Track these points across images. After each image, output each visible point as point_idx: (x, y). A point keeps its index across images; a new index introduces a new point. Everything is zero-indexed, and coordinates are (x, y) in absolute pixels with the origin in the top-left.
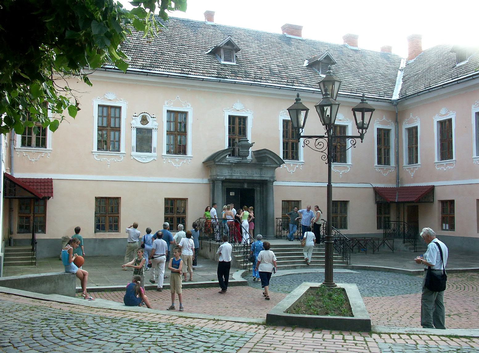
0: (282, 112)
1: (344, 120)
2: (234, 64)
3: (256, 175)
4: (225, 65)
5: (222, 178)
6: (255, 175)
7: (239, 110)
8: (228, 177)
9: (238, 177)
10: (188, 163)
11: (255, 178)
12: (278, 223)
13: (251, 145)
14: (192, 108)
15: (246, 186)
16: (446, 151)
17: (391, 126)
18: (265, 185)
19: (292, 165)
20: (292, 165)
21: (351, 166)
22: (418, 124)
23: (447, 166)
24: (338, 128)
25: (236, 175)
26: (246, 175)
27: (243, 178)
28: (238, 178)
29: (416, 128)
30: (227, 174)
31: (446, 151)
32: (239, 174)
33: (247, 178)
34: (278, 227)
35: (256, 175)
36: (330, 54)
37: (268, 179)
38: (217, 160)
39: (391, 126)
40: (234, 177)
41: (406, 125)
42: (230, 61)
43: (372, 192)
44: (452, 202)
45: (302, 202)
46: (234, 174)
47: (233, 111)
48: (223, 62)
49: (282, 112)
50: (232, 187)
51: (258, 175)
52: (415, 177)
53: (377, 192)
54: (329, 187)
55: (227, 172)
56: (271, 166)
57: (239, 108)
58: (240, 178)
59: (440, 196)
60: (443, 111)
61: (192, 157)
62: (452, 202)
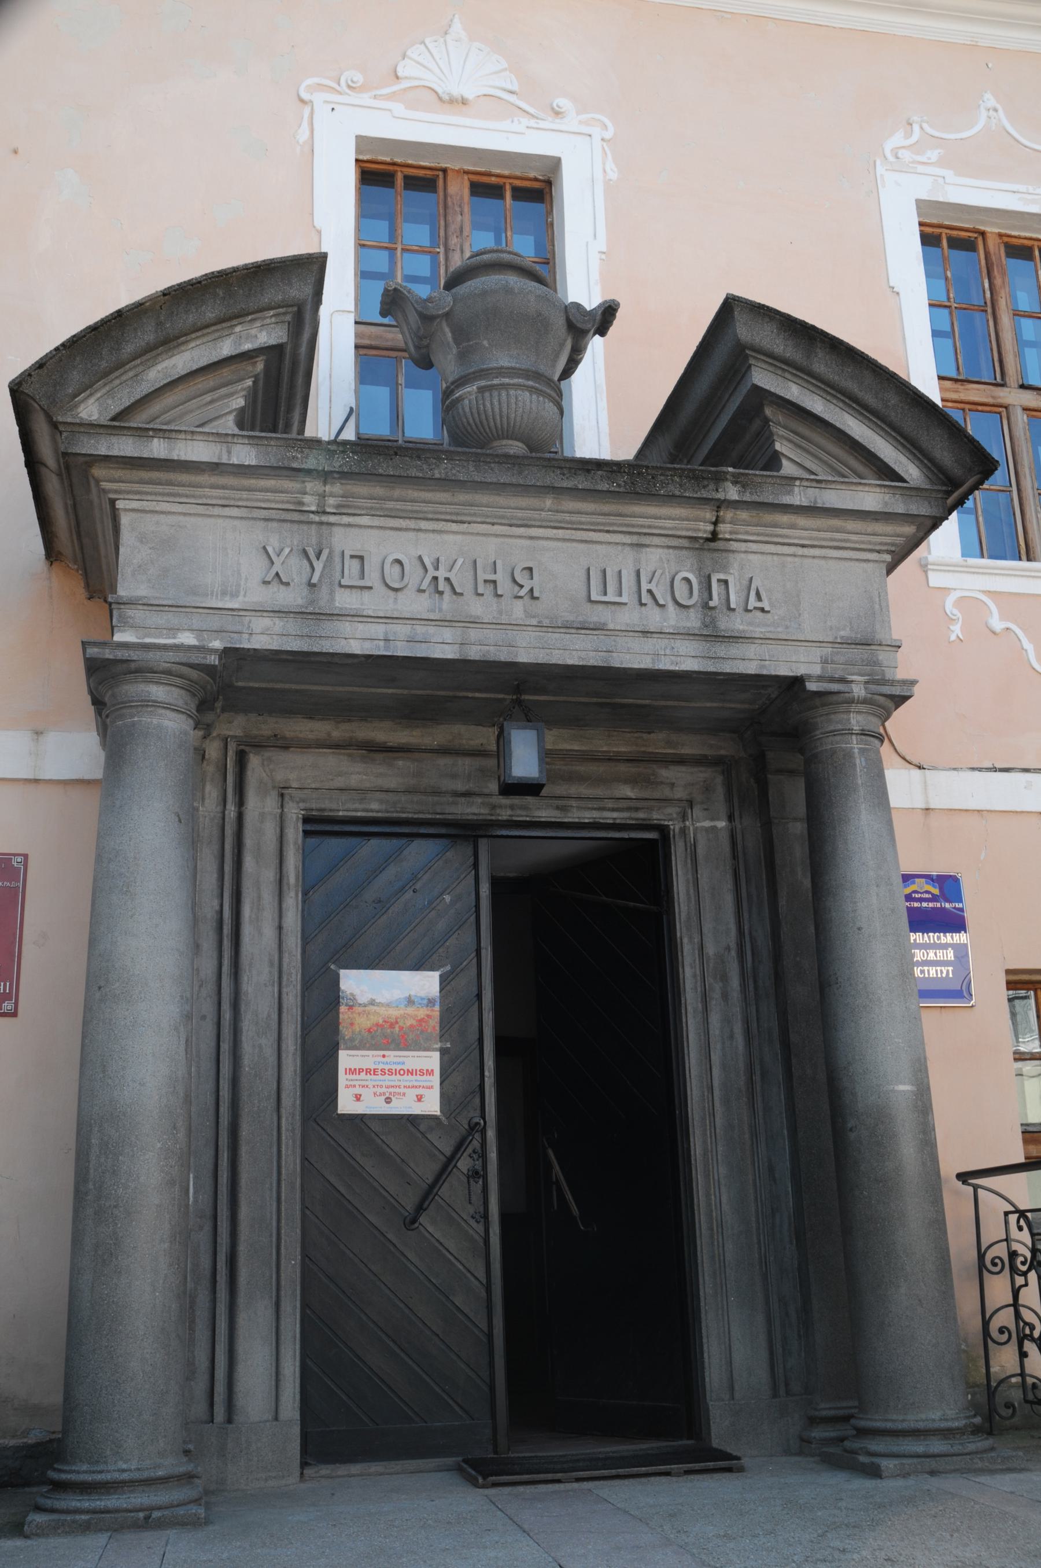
0: (897, 139)
5: (187, 639)
6: (604, 597)
7: (464, 102)
8: (264, 635)
9: (402, 630)
11: (635, 655)
12: (993, 1231)
27: (474, 653)
28: (401, 650)
30: (256, 595)
34: (999, 1289)
40: (356, 640)
46: (345, 600)
47: (398, 108)
51: (672, 618)
55: (253, 568)
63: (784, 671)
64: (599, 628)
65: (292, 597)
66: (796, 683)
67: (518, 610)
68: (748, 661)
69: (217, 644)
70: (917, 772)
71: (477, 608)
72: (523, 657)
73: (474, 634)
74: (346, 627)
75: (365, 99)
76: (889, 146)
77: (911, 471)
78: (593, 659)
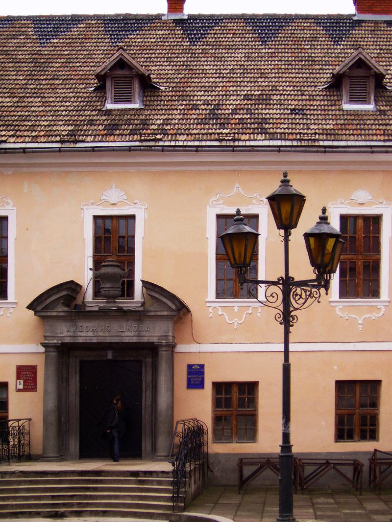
0: (214, 199)
1: (370, 204)
2: (136, 106)
3: (129, 334)
4: (109, 112)
5: (55, 341)
8: (67, 340)
9: (88, 338)
10: (9, 315)
11: (127, 340)
14: (15, 208)
15: (110, 355)
19: (236, 309)
20: (236, 309)
21: (387, 304)
24: (360, 222)
25: (83, 334)
26: (107, 334)
27: (100, 341)
28: (88, 341)
30: (65, 334)
32: (90, 334)
33: (108, 340)
35: (129, 334)
36: (369, 59)
37: (155, 340)
38: (39, 308)
40: (80, 340)
42: (129, 101)
45: (261, 387)
46: (79, 334)
48: (109, 106)
49: (214, 199)
50: (91, 359)
51: (133, 333)
54: (287, 352)
55: (65, 329)
56: (159, 313)
57: (114, 199)
58: (94, 341)
61: (16, 303)
63: (151, 341)
64: (120, 336)
65: (71, 334)
66: (153, 343)
67: (107, 334)
68: (145, 340)
69: (60, 342)
70: (198, 345)
71: (101, 334)
72: (108, 341)
73: (99, 338)
74: (79, 338)
75: (94, 206)
76: (210, 202)
77: (174, 307)
78: (119, 341)
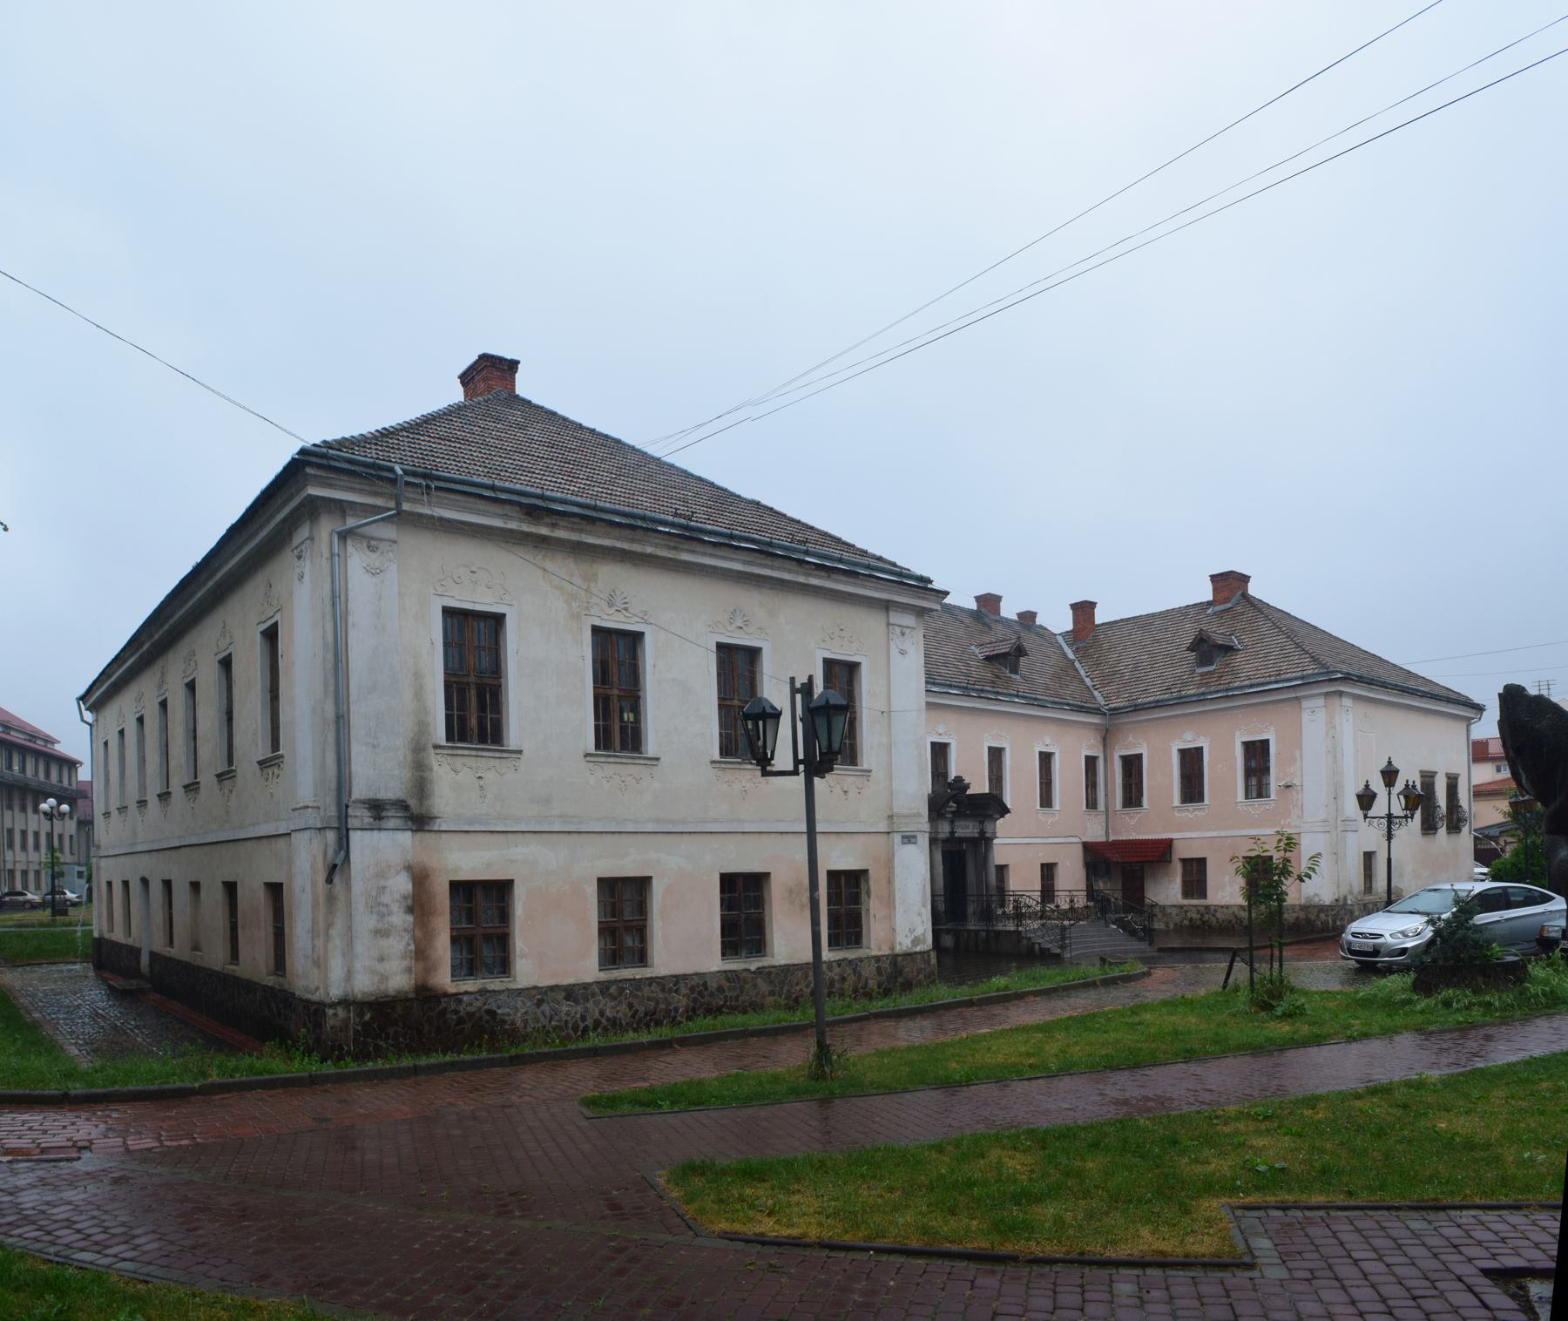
13: (967, 786)
16: (1192, 788)
17: (1097, 752)
18: (983, 842)
22: (1143, 749)
23: (1192, 812)
29: (1139, 756)
31: (1192, 788)
39: (1097, 752)
41: (1120, 751)
43: (1079, 849)
44: (1202, 862)
52: (1137, 827)
53: (1088, 848)
59: (1182, 851)
60: (1189, 736)
62: (1202, 862)
